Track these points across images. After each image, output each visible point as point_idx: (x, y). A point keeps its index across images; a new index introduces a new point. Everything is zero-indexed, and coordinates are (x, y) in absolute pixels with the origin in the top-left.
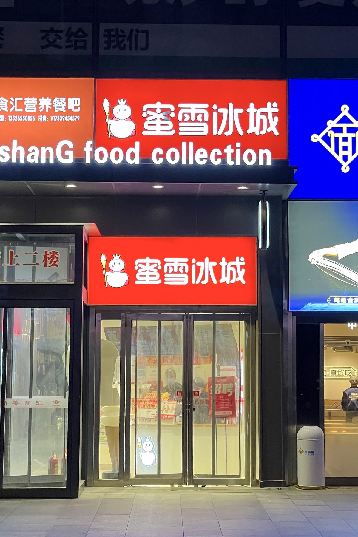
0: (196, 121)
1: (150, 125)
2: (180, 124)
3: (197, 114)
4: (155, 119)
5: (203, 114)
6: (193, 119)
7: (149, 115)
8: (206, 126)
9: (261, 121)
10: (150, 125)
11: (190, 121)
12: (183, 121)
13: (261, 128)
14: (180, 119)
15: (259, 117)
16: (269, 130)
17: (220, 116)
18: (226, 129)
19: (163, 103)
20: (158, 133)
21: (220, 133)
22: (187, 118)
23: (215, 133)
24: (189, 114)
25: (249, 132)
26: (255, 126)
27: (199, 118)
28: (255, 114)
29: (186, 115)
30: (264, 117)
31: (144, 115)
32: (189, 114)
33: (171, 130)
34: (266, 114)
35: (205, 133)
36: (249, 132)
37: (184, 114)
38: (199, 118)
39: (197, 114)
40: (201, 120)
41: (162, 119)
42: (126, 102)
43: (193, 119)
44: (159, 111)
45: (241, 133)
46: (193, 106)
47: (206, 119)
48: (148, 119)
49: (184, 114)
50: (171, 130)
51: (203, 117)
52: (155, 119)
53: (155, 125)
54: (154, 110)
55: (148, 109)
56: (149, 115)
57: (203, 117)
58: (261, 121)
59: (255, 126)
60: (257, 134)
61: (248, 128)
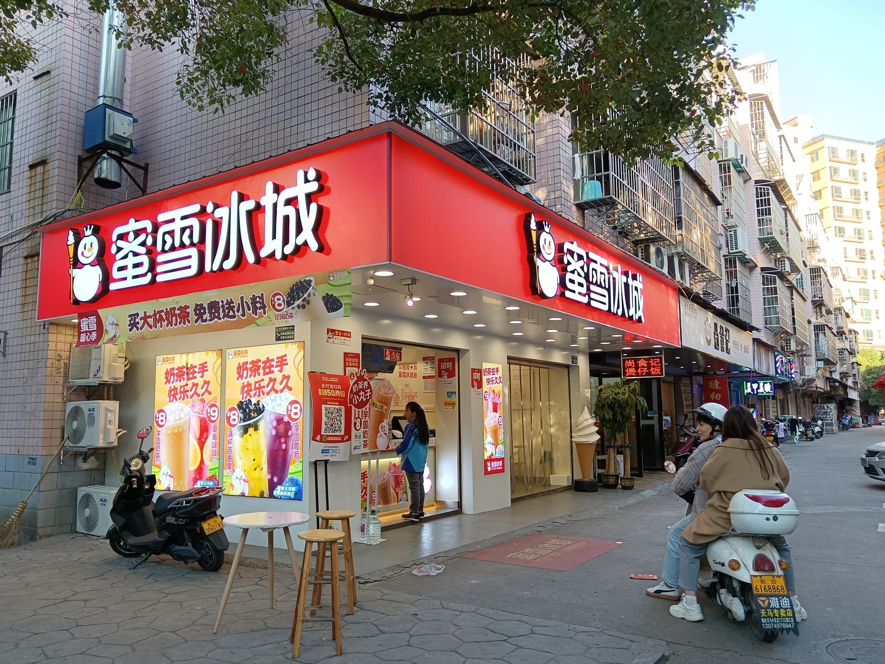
0: (183, 246)
2: (160, 258)
3: (183, 230)
4: (126, 257)
5: (191, 227)
6: (177, 244)
8: (193, 252)
9: (286, 219)
11: (173, 249)
12: (164, 251)
13: (286, 241)
16: (300, 241)
17: (217, 225)
18: (226, 256)
21: (216, 267)
23: (208, 269)
25: (264, 253)
26: (274, 237)
28: (275, 206)
29: (167, 237)
30: (290, 211)
31: (114, 250)
32: (171, 233)
33: (145, 275)
34: (292, 202)
35: (193, 271)
36: (264, 253)
39: (183, 230)
41: (136, 254)
44: (131, 236)
46: (177, 213)
47: (196, 239)
50: (145, 275)
51: (191, 236)
52: (126, 257)
56: (119, 249)
57: (191, 236)
58: (286, 219)
59: (274, 237)
60: (278, 256)
61: (262, 246)
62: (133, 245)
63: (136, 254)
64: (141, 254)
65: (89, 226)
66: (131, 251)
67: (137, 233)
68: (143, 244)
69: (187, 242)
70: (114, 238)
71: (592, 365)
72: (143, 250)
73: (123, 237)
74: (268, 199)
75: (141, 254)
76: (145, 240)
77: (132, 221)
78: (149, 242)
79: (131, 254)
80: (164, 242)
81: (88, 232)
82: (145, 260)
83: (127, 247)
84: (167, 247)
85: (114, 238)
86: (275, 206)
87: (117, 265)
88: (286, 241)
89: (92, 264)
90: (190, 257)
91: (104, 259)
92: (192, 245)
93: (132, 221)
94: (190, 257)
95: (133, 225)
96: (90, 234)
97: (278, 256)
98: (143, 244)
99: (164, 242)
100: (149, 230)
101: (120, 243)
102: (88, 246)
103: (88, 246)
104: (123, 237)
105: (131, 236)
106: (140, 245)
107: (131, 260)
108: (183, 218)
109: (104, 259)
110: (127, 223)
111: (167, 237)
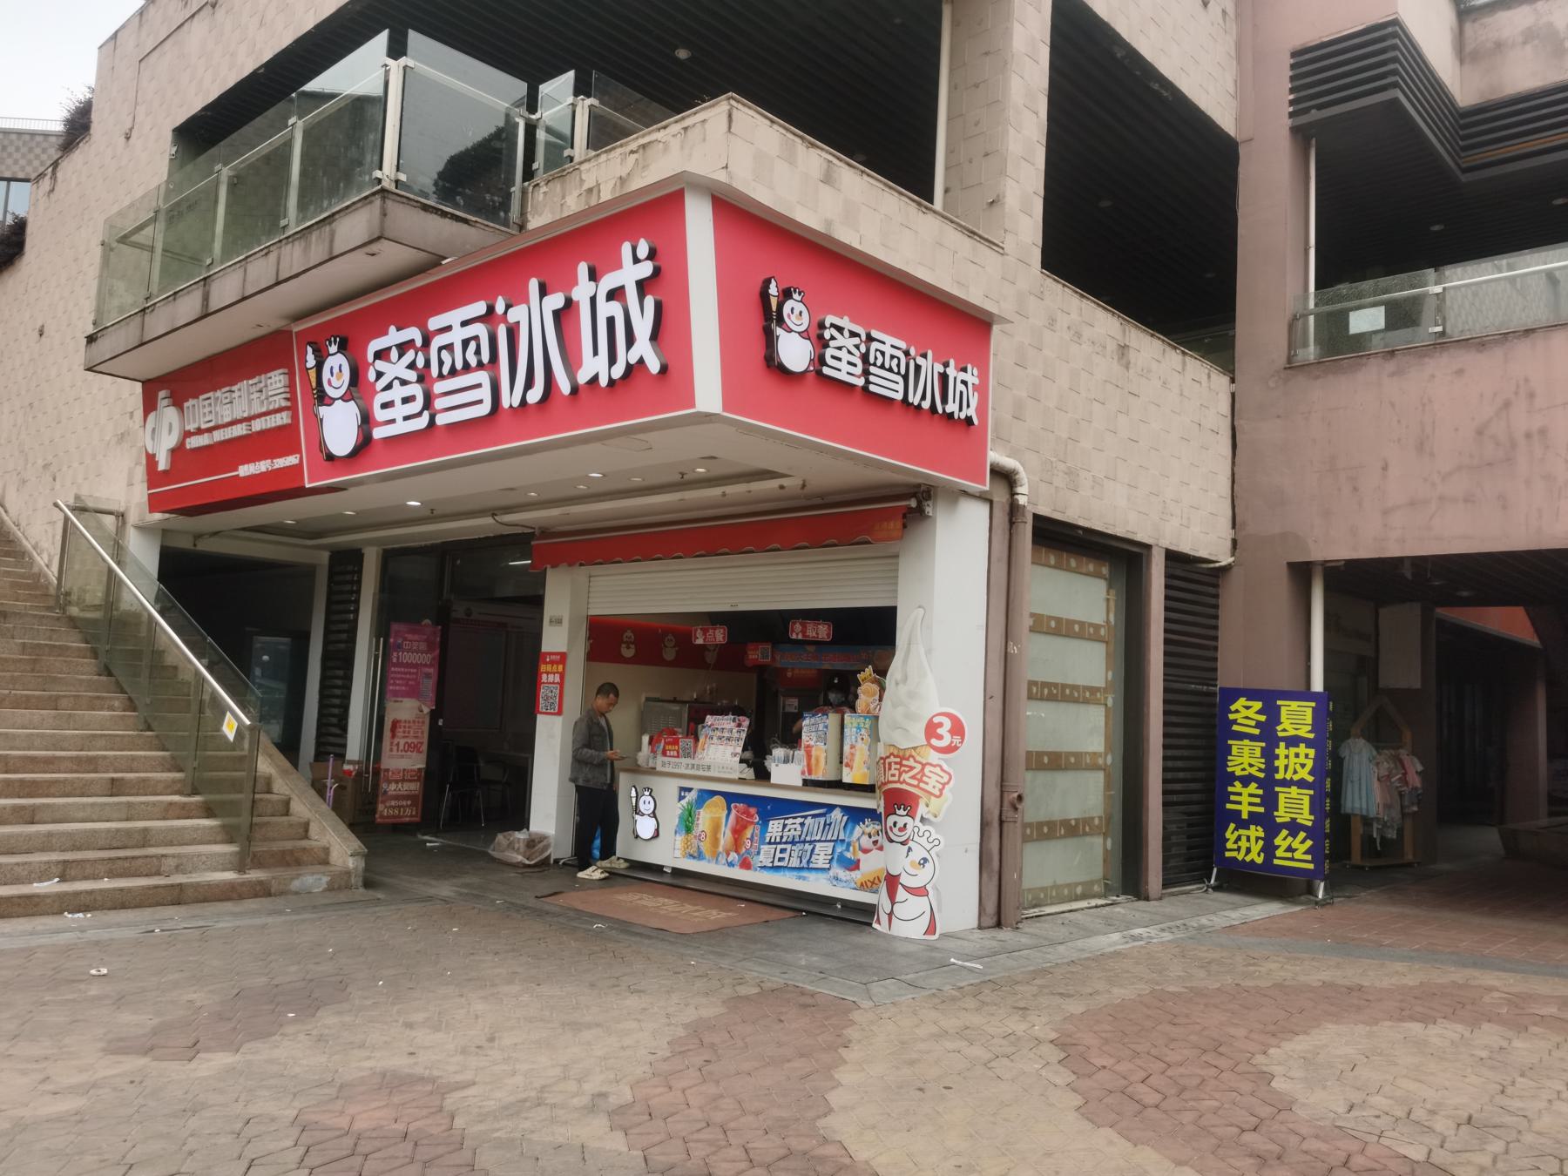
0: (467, 368)
2: (439, 387)
6: (459, 365)
11: (453, 372)
12: (441, 376)
13: (612, 360)
14: (435, 372)
25: (583, 377)
26: (596, 353)
29: (445, 355)
31: (372, 376)
37: (440, 349)
41: (404, 383)
44: (394, 354)
47: (485, 358)
51: (478, 352)
56: (379, 375)
57: (478, 352)
59: (596, 353)
60: (603, 382)
61: (580, 365)
62: (396, 368)
63: (404, 383)
64: (411, 383)
65: (333, 339)
66: (396, 378)
67: (403, 348)
68: (412, 366)
69: (473, 361)
70: (370, 358)
71: (1168, 602)
73: (382, 355)
75: (411, 383)
76: (415, 360)
77: (392, 329)
78: (420, 363)
79: (396, 383)
80: (441, 363)
81: (333, 349)
82: (416, 390)
84: (445, 371)
85: (370, 358)
87: (381, 398)
88: (612, 360)
89: (344, 398)
91: (358, 385)
92: (480, 365)
93: (392, 329)
95: (394, 337)
96: (336, 350)
97: (603, 382)
98: (412, 366)
99: (441, 363)
100: (419, 343)
101: (380, 365)
102: (336, 370)
103: (336, 370)
104: (382, 355)
105: (394, 354)
108: (464, 324)
109: (358, 385)
110: (385, 333)
111: (445, 355)
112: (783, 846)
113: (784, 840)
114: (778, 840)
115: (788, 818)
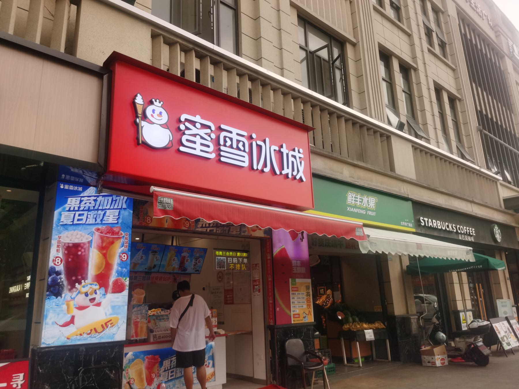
0: (238, 148)
1: (188, 140)
3: (238, 141)
6: (235, 146)
7: (187, 128)
9: (293, 162)
10: (188, 140)
11: (231, 147)
12: (225, 145)
14: (222, 142)
15: (291, 159)
18: (265, 165)
19: (202, 118)
20: (197, 152)
22: (229, 143)
24: (231, 139)
25: (284, 172)
26: (288, 168)
27: (240, 145)
28: (287, 155)
29: (227, 139)
36: (284, 172)
37: (225, 137)
38: (240, 145)
40: (242, 149)
41: (202, 138)
42: (162, 104)
43: (235, 146)
44: (198, 126)
45: (278, 172)
46: (235, 131)
47: (247, 150)
48: (187, 132)
49: (225, 137)
50: (211, 153)
51: (244, 145)
52: (195, 135)
53: (194, 142)
54: (193, 123)
55: (187, 120)
56: (187, 128)
57: (244, 145)
58: (293, 162)
59: (288, 168)
63: (202, 138)
67: (204, 126)
72: (209, 139)
74: (284, 150)
80: (225, 141)
83: (194, 131)
86: (287, 155)
90: (244, 157)
92: (244, 151)
94: (244, 157)
99: (225, 141)
101: (188, 124)
106: (206, 134)
107: (198, 139)
112: (172, 370)
113: (172, 367)
114: (169, 368)
115: (172, 358)
